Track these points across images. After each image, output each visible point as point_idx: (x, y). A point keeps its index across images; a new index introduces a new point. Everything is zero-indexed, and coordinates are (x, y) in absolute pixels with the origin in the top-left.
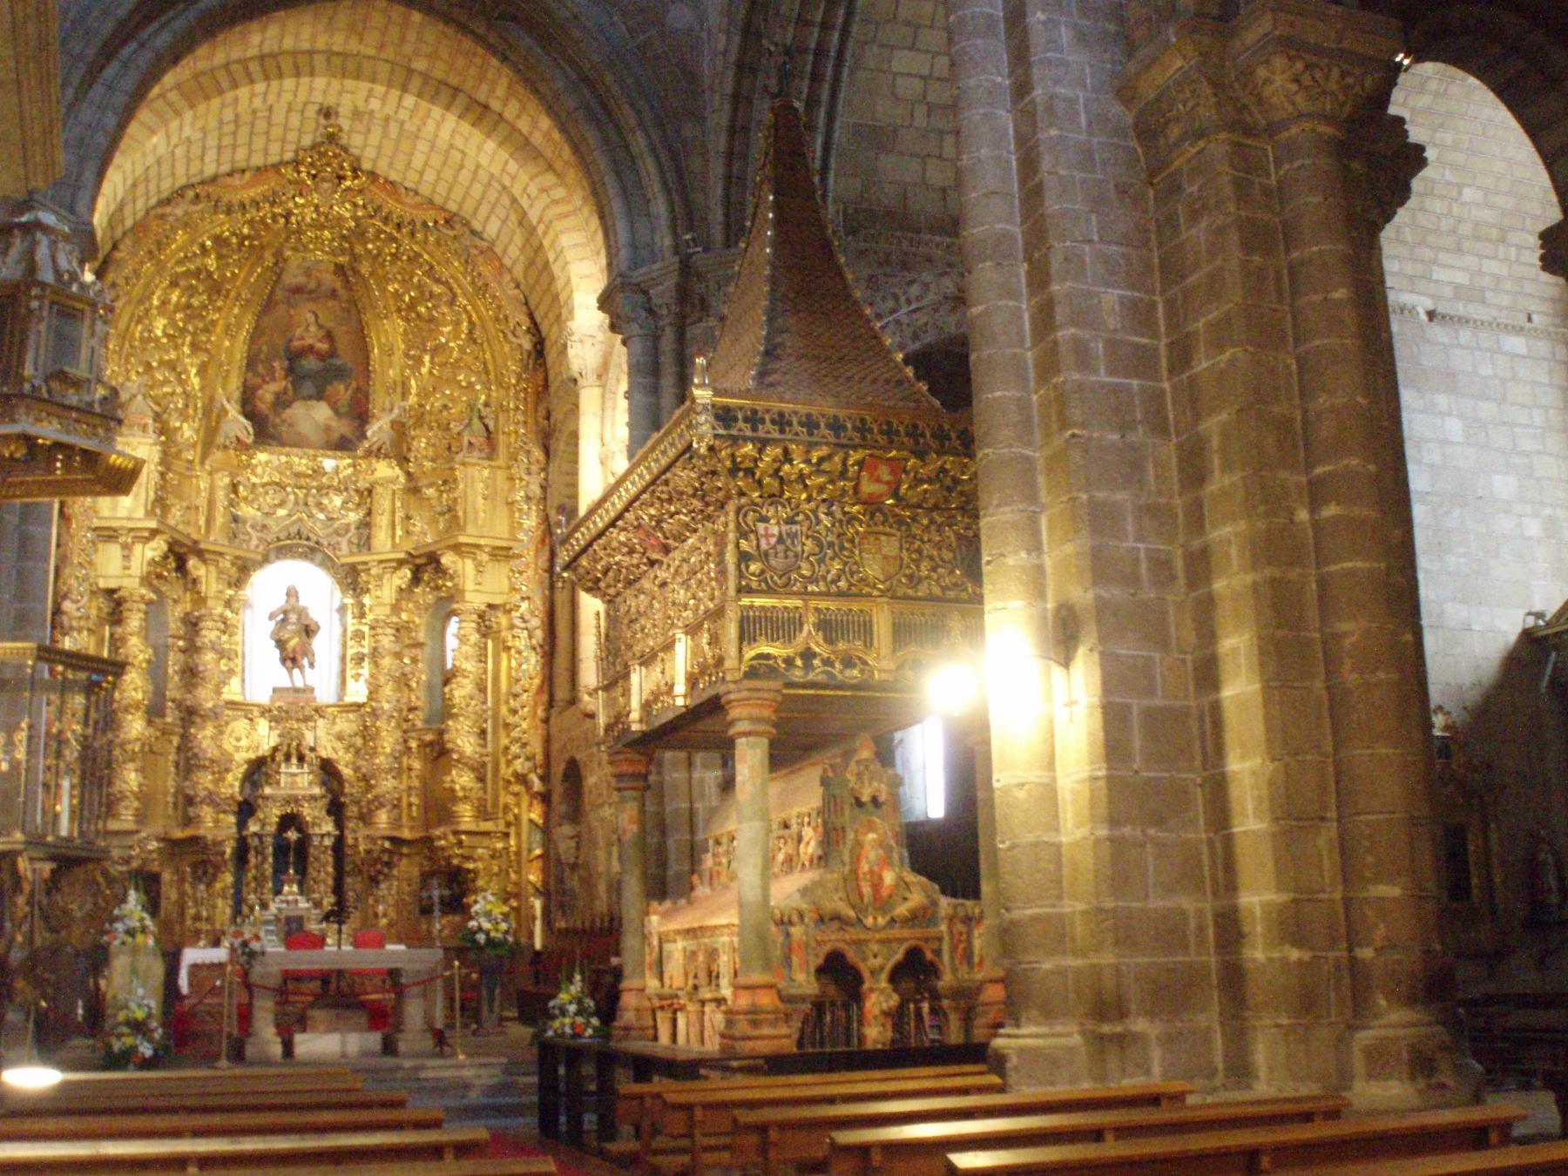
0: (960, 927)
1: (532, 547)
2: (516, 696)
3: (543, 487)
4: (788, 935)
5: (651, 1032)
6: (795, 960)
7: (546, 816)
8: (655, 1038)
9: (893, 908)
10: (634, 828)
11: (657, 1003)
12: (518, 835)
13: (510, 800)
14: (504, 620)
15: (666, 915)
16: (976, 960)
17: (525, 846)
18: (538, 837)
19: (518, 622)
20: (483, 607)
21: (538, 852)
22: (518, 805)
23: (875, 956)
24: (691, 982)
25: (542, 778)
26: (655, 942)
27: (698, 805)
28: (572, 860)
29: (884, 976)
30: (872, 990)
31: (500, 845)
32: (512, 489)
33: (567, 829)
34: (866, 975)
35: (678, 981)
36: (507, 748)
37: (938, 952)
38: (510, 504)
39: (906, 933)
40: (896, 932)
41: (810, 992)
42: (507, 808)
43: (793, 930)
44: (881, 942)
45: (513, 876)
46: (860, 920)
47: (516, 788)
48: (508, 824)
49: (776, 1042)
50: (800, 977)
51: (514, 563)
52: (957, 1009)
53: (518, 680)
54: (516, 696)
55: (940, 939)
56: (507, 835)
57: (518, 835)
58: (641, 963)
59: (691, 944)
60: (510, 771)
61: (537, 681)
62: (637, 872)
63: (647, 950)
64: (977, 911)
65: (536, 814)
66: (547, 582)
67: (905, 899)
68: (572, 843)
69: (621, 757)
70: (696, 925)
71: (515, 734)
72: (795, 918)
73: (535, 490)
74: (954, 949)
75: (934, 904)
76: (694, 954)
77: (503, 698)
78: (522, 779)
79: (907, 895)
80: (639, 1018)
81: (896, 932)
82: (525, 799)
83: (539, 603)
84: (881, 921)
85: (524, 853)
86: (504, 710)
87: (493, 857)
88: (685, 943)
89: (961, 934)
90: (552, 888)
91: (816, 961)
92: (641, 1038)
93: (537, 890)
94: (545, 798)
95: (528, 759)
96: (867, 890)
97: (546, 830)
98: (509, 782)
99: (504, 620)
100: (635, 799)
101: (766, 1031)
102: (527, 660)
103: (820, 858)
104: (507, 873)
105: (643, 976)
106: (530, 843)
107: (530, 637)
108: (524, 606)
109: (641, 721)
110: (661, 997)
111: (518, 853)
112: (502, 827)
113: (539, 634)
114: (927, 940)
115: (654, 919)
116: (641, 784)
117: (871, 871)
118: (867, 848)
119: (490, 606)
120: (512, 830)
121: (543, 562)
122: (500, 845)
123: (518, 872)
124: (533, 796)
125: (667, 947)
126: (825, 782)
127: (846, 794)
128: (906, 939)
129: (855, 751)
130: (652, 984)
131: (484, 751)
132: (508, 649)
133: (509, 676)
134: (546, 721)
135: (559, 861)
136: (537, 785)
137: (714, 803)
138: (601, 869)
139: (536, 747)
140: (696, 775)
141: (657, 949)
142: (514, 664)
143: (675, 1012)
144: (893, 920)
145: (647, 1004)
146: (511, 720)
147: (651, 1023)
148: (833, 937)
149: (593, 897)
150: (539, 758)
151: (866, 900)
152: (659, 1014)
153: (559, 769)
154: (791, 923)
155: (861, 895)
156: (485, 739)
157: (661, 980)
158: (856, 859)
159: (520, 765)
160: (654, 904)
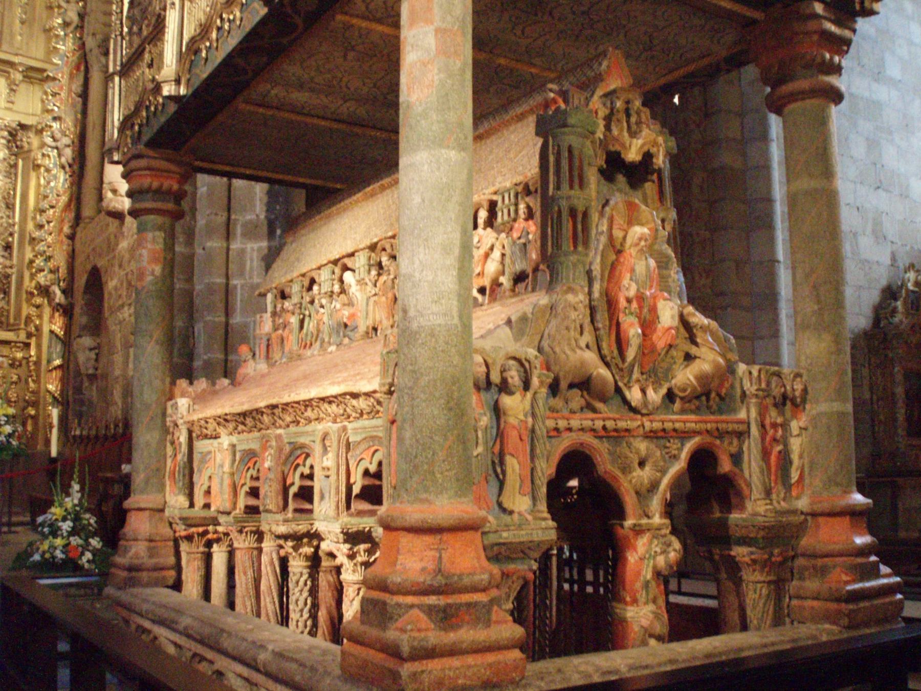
0: (773, 415)
1: (66, 70)
2: (42, 211)
3: (79, 15)
4: (497, 411)
5: (172, 573)
6: (513, 465)
7: (68, 328)
8: (177, 586)
9: (668, 374)
10: (158, 269)
11: (181, 531)
12: (39, 346)
13: (33, 311)
14: (35, 141)
15: (200, 399)
16: (795, 476)
17: (44, 357)
18: (59, 348)
19: (49, 141)
20: (14, 125)
21: (58, 362)
22: (40, 317)
23: (642, 464)
24: (242, 502)
25: (64, 292)
26: (183, 438)
27: (234, 282)
28: (91, 371)
29: (656, 504)
30: (638, 531)
31: (19, 355)
32: (51, 17)
33: (87, 341)
34: (630, 501)
35: (221, 500)
36: (31, 262)
37: (737, 458)
38: (48, 31)
39: (690, 421)
40: (675, 419)
41: (538, 536)
42: (28, 319)
43: (507, 401)
44: (651, 436)
45: (32, 385)
46: (618, 390)
47: (38, 300)
48: (29, 335)
49: (491, 658)
50: (520, 503)
51: (49, 87)
52: (766, 565)
53: (46, 197)
54: (42, 211)
55: (742, 435)
56: (27, 345)
57: (39, 346)
58: (159, 471)
59: (248, 441)
60: (33, 284)
61: (64, 199)
62: (158, 334)
63: (169, 450)
64: (798, 387)
65: (58, 326)
66: (79, 107)
67: (689, 358)
68: (93, 355)
69: (143, 163)
70: (262, 404)
71: (41, 247)
72: (514, 377)
73: (73, 16)
74: (766, 454)
75: (731, 369)
76: (251, 456)
77: (30, 215)
78: (45, 291)
79: (694, 350)
80: (152, 552)
81: (675, 419)
82: (47, 311)
83: (69, 122)
84: (655, 396)
85: (44, 362)
86: (30, 226)
87: (12, 365)
88: (234, 439)
89: (774, 425)
90: (71, 399)
91: (546, 469)
92: (157, 583)
93: (55, 398)
94: (67, 311)
95: (51, 271)
96: (633, 331)
97: (67, 342)
98: (32, 294)
99: (35, 141)
100: (160, 228)
101: (466, 635)
102: (55, 177)
103: (519, 278)
104: (27, 382)
105: (162, 488)
106: (50, 354)
107: (60, 155)
108: (56, 125)
109: (178, 81)
110: (188, 522)
111: (37, 363)
112: (23, 336)
113: (68, 152)
114: (721, 434)
115: (183, 403)
116: (170, 206)
117: (640, 298)
118: (631, 251)
119: (23, 127)
120: (33, 341)
121: (77, 86)
122: (19, 355)
123: (37, 381)
124: (56, 308)
125: (201, 446)
126: (543, 129)
127: (589, 150)
128: (699, 433)
129: (599, 79)
130: (176, 501)
131: (8, 263)
132: (39, 166)
133: (38, 194)
134: (72, 237)
135: (78, 373)
136: (59, 297)
137: (256, 280)
138: (117, 372)
139: (60, 260)
140: (235, 246)
141: (184, 448)
142: (42, 181)
143: (209, 544)
144: (670, 396)
145: (168, 532)
146: (37, 234)
147: (172, 560)
148: (575, 423)
149: (108, 404)
150: (63, 272)
151: (631, 354)
152: (184, 547)
153: (81, 281)
154: (504, 387)
155: (621, 344)
156: (11, 254)
157: (191, 496)
158: (612, 271)
159: (42, 278)
160: (183, 383)
